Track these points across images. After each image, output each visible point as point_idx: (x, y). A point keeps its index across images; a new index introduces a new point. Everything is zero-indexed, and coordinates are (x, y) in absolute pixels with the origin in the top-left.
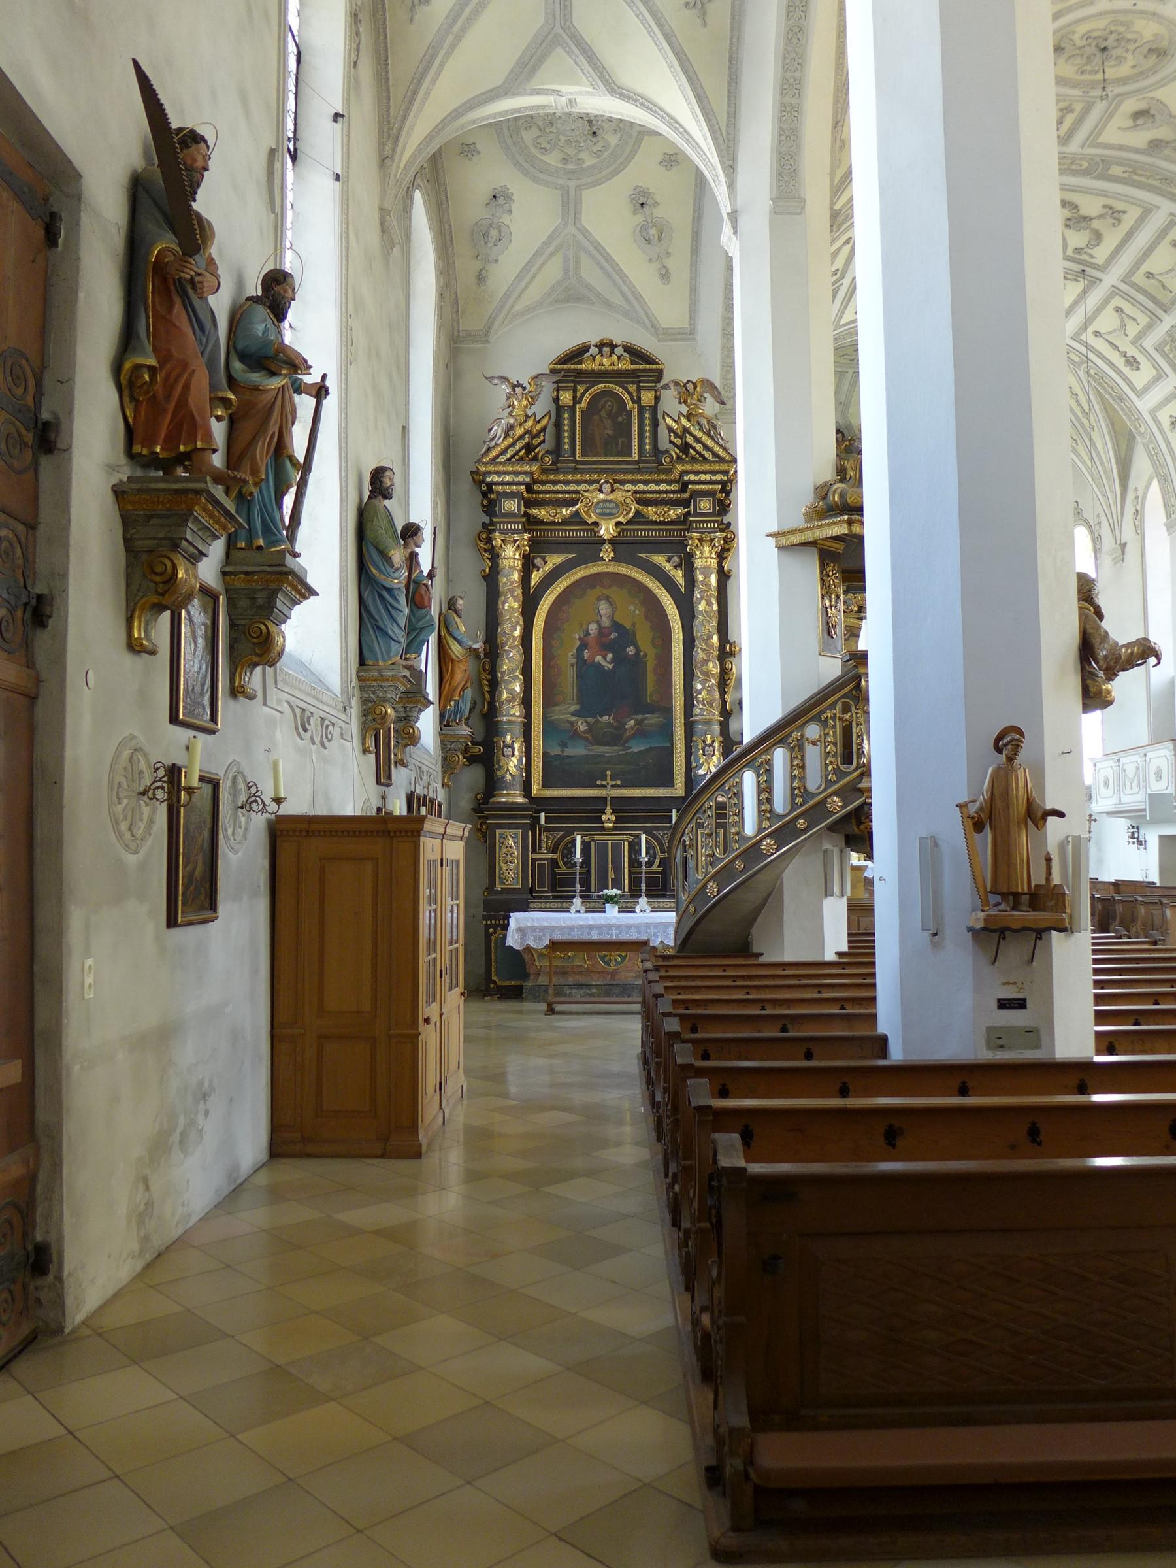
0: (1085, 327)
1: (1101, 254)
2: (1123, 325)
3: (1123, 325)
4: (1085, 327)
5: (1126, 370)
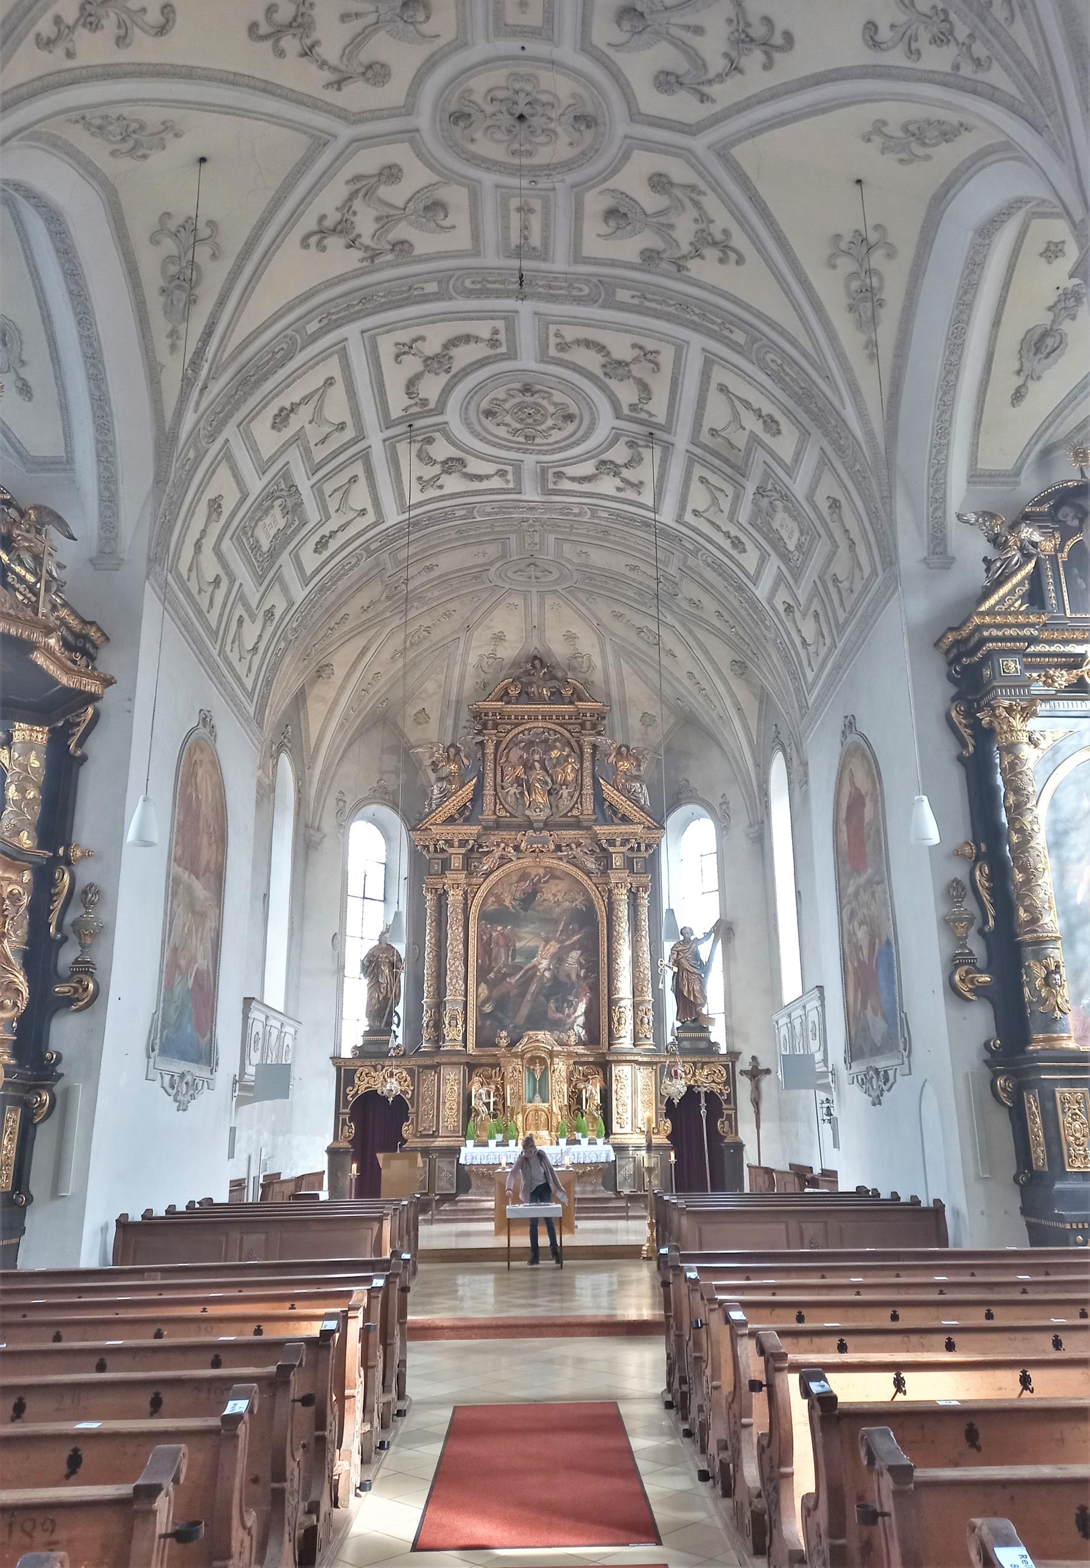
0: (682, 508)
1: (658, 408)
2: (715, 500)
3: (715, 500)
4: (682, 508)
5: (734, 553)
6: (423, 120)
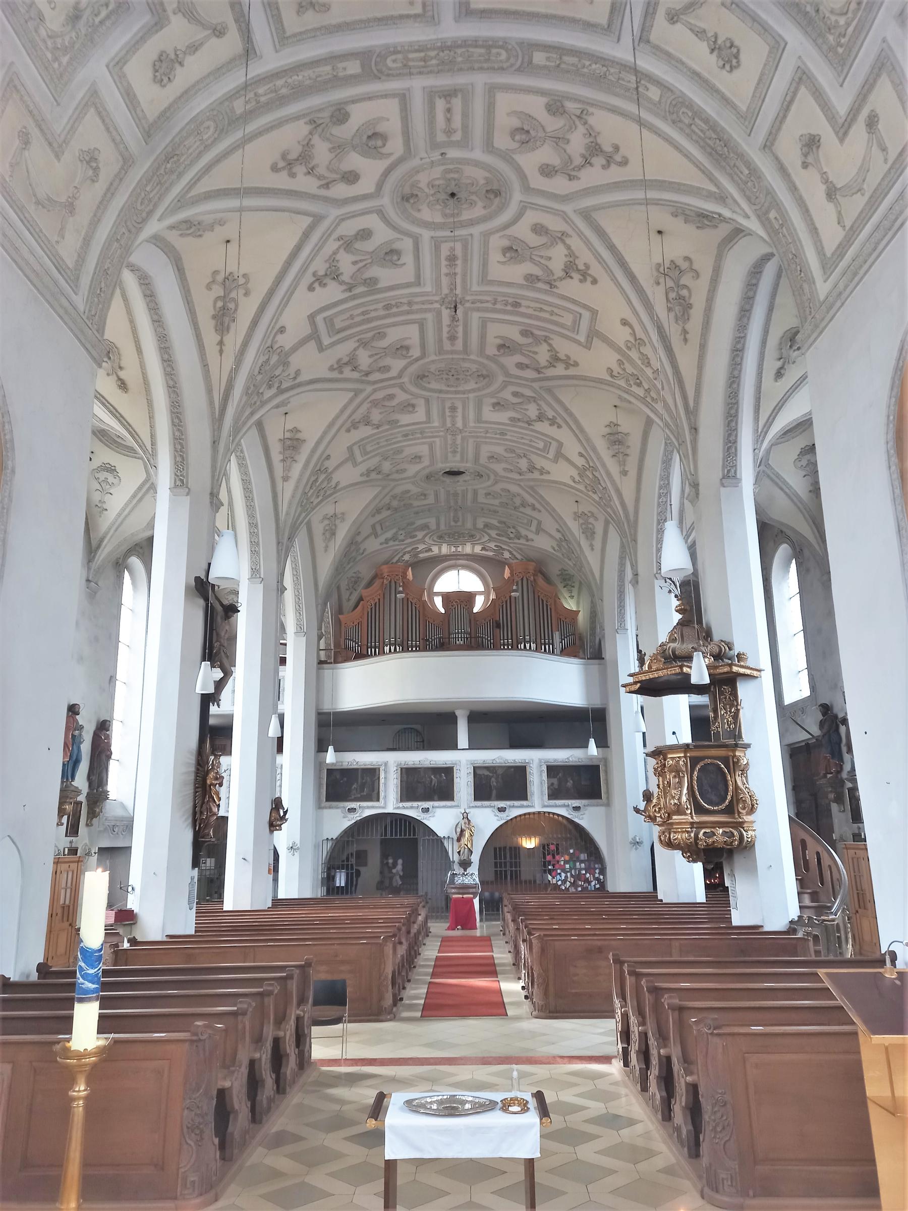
6: (517, 196)
